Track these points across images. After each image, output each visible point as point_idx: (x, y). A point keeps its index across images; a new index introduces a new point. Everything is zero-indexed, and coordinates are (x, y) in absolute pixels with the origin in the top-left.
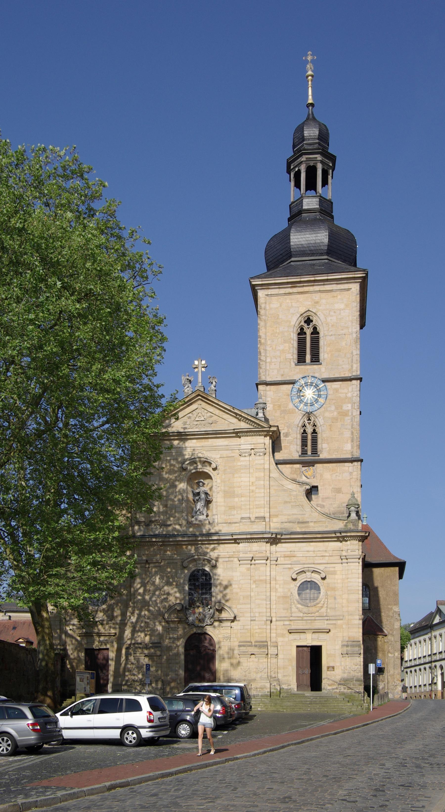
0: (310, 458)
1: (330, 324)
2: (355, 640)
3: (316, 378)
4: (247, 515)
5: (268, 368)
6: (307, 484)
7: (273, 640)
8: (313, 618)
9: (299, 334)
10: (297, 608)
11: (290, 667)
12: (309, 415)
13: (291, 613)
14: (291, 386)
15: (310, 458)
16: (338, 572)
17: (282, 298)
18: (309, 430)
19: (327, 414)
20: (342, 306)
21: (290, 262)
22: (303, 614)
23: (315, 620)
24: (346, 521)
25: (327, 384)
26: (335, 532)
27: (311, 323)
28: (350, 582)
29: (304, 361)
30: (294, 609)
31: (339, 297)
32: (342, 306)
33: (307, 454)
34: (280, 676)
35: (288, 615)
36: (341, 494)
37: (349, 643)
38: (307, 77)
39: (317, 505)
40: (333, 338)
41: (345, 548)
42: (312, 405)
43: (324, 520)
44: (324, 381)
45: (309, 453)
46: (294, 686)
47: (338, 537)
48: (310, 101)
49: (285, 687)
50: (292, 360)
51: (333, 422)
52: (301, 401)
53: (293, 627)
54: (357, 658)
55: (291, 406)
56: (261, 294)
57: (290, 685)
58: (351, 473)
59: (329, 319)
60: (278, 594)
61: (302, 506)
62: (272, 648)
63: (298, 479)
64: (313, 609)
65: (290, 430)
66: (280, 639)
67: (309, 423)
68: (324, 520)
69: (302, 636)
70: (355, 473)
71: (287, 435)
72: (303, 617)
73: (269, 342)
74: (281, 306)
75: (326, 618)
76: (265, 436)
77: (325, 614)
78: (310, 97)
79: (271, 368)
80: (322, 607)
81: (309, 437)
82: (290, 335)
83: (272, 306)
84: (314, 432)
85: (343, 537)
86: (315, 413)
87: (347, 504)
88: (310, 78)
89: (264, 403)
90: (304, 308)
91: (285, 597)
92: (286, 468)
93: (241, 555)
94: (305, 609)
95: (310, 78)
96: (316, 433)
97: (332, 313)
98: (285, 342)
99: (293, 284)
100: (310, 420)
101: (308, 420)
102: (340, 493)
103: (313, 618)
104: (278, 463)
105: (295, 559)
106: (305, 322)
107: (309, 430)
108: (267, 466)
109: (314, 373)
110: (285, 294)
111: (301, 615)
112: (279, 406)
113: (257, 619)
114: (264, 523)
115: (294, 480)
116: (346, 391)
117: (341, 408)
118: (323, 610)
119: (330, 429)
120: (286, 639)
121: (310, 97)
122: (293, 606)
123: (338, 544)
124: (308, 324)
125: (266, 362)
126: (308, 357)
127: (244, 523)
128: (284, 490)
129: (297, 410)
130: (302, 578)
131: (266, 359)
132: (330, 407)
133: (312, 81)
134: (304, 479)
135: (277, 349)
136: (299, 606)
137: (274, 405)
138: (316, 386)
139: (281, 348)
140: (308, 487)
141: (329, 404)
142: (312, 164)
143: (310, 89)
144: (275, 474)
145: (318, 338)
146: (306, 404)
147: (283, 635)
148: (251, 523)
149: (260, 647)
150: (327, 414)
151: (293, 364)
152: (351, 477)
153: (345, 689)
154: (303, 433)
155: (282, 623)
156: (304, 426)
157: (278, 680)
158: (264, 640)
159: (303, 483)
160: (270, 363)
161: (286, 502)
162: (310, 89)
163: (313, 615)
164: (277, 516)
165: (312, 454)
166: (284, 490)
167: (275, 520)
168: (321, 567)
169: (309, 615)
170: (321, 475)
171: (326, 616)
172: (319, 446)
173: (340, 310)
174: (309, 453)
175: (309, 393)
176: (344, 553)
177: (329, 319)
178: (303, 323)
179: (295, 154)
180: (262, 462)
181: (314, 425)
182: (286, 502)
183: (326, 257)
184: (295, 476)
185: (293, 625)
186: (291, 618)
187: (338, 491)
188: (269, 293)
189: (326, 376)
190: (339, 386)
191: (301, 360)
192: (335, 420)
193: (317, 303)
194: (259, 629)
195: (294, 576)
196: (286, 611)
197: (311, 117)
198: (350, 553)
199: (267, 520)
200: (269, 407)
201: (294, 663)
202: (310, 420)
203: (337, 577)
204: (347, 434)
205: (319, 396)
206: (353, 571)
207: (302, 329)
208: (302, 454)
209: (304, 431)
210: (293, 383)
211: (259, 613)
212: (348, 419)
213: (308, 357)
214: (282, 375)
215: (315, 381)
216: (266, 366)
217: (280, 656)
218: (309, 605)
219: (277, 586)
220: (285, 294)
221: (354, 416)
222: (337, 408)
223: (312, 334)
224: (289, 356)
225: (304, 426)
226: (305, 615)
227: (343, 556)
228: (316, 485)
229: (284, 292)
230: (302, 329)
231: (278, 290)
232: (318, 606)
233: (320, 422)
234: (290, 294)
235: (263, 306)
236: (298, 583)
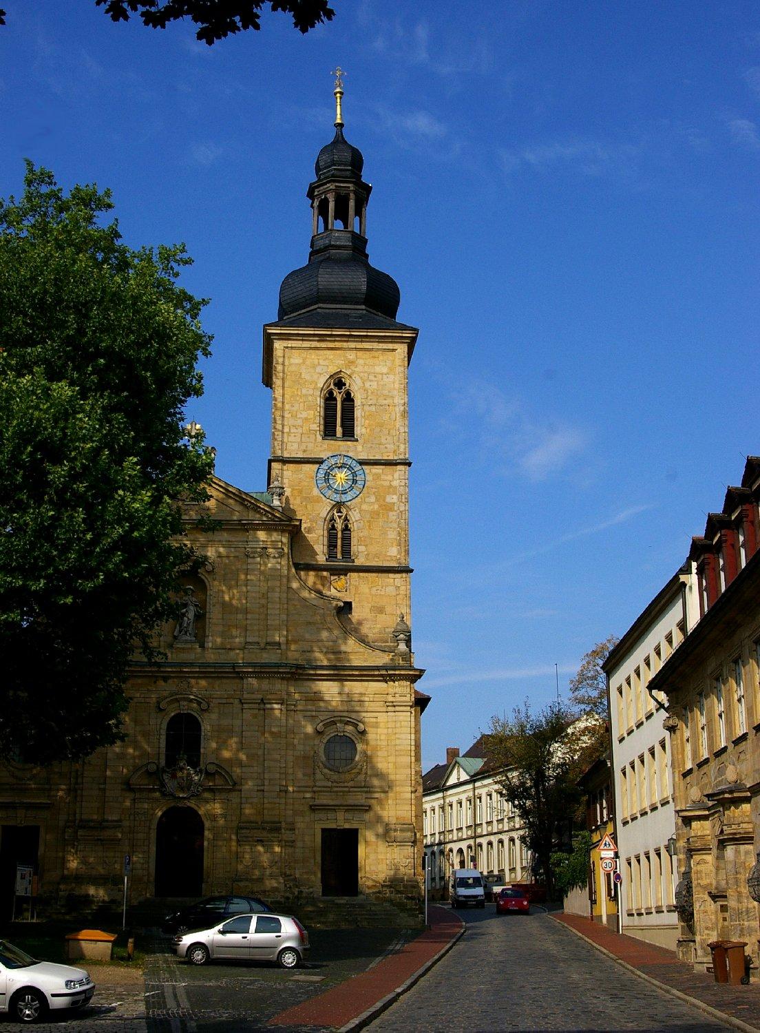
0: (341, 563)
1: (370, 391)
2: (406, 822)
3: (351, 458)
4: (256, 639)
5: (285, 440)
6: (339, 600)
7: (290, 820)
8: (347, 789)
10: (324, 775)
11: (312, 861)
12: (339, 506)
13: (314, 781)
14: (317, 466)
15: (341, 563)
16: (382, 725)
17: (304, 354)
19: (364, 507)
21: (316, 309)
22: (332, 782)
23: (349, 792)
24: (393, 654)
25: (364, 467)
26: (378, 668)
27: (344, 387)
28: (399, 739)
30: (319, 776)
33: (336, 557)
35: (311, 784)
36: (383, 615)
37: (397, 826)
38: (336, 94)
41: (391, 691)
42: (344, 492)
43: (362, 650)
44: (362, 463)
45: (339, 556)
46: (318, 889)
47: (382, 675)
48: (339, 121)
50: (318, 432)
51: (372, 518)
53: (317, 802)
54: (409, 848)
55: (316, 492)
56: (278, 345)
57: (312, 888)
58: (398, 588)
60: (298, 754)
62: (288, 832)
63: (324, 592)
64: (348, 776)
65: (314, 525)
66: (298, 819)
67: (340, 517)
68: (362, 650)
69: (331, 815)
70: (403, 588)
71: (309, 530)
72: (331, 787)
73: (287, 407)
74: (304, 363)
75: (366, 789)
77: (363, 784)
78: (339, 116)
79: (290, 440)
80: (359, 773)
81: (339, 535)
82: (316, 400)
83: (292, 361)
84: (346, 529)
85: (390, 675)
86: (349, 503)
87: (393, 630)
88: (338, 95)
89: (280, 488)
90: (336, 368)
91: (305, 758)
93: (245, 696)
94: (335, 777)
95: (338, 95)
96: (350, 530)
97: (371, 377)
98: (309, 408)
99: (322, 338)
100: (342, 512)
101: (337, 512)
102: (382, 613)
103: (347, 789)
106: (335, 385)
107: (339, 525)
109: (348, 451)
110: (311, 348)
111: (330, 784)
112: (300, 492)
113: (266, 788)
114: (279, 651)
116: (390, 477)
117: (384, 501)
118: (362, 777)
119: (369, 526)
121: (339, 116)
122: (318, 771)
123: (383, 685)
124: (340, 388)
125: (283, 433)
126: (339, 430)
127: (251, 650)
129: (324, 498)
130: (331, 732)
131: (283, 428)
132: (368, 497)
133: (341, 98)
135: (298, 417)
136: (326, 771)
137: (293, 489)
138: (350, 468)
139: (304, 415)
141: (368, 493)
142: (343, 192)
143: (338, 107)
145: (353, 407)
146: (336, 491)
148: (260, 651)
149: (272, 830)
150: (364, 507)
151: (319, 438)
152: (398, 593)
153: (391, 892)
154: (331, 530)
158: (277, 820)
160: (289, 433)
162: (338, 107)
163: (346, 784)
165: (343, 558)
167: (293, 647)
169: (341, 784)
170: (357, 588)
171: (364, 787)
172: (354, 549)
174: (339, 556)
175: (341, 477)
176: (390, 698)
177: (367, 384)
178: (332, 386)
179: (319, 180)
181: (346, 519)
183: (363, 307)
185: (318, 799)
186: (315, 789)
187: (381, 610)
188: (289, 346)
189: (363, 456)
190: (381, 471)
191: (329, 432)
192: (375, 515)
193: (352, 362)
194: (269, 803)
196: (306, 778)
197: (340, 138)
198: (398, 699)
199: (283, 647)
200: (288, 492)
202: (342, 512)
203: (379, 730)
204: (392, 535)
205: (354, 481)
206: (403, 723)
207: (331, 393)
208: (329, 557)
209: (333, 526)
210: (320, 462)
211: (270, 780)
212: (393, 516)
213: (339, 430)
214: (304, 451)
215: (349, 462)
216: (283, 437)
217: (299, 844)
218: (341, 771)
220: (311, 348)
221: (401, 512)
222: (377, 500)
223: (343, 401)
224: (315, 427)
225: (332, 519)
226: (335, 784)
227: (389, 702)
228: (349, 600)
229: (309, 346)
230: (331, 393)
231: (301, 342)
232: (353, 771)
235: (280, 360)
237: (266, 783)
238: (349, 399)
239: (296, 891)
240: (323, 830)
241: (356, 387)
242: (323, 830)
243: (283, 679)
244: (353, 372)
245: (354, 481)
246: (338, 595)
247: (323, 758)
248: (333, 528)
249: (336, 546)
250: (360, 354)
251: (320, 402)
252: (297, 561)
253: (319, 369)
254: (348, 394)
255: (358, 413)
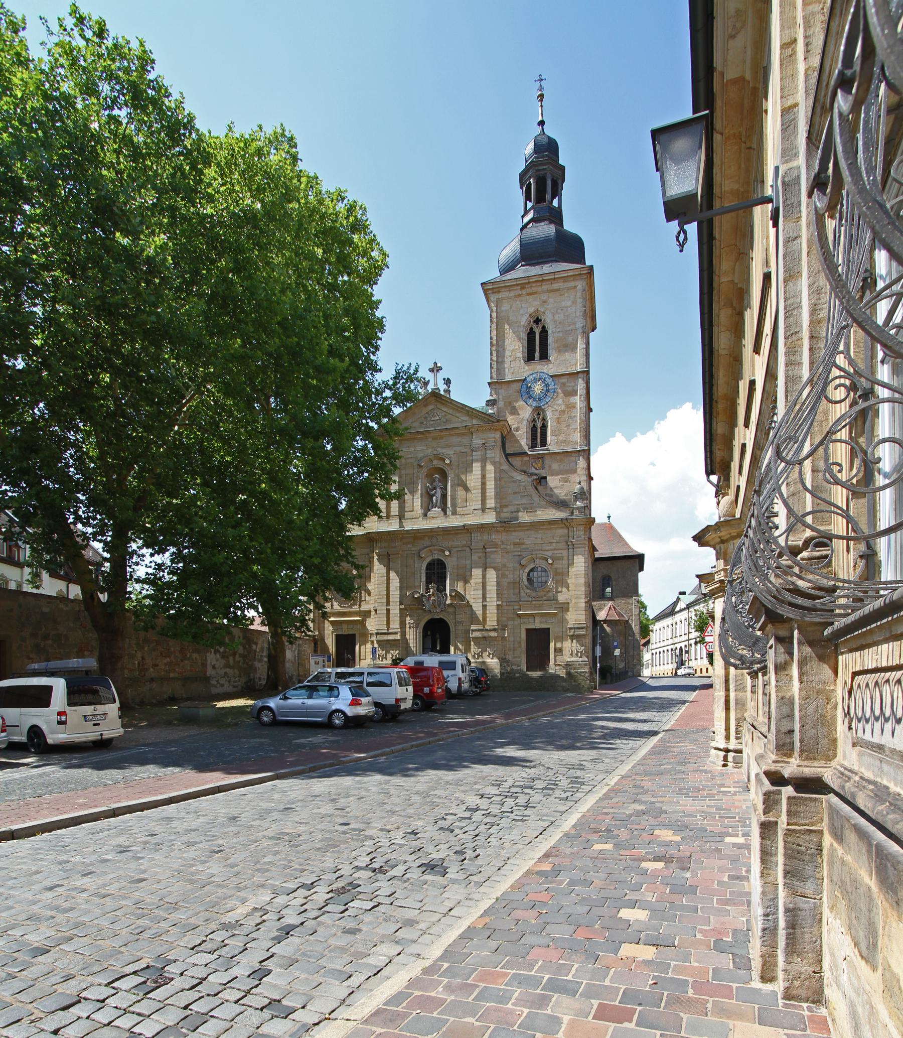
6: (536, 474)
9: (529, 334)
18: (539, 424)
20: (569, 303)
29: (534, 360)
30: (523, 594)
31: (566, 295)
32: (569, 303)
34: (509, 657)
35: (517, 599)
39: (546, 495)
40: (561, 334)
42: (540, 399)
44: (552, 376)
49: (515, 668)
52: (530, 397)
59: (556, 317)
61: (531, 496)
64: (542, 594)
69: (531, 620)
71: (517, 429)
76: (496, 430)
81: (539, 431)
83: (503, 308)
91: (514, 583)
92: (517, 461)
94: (534, 594)
97: (559, 311)
104: (507, 456)
105: (524, 546)
106: (534, 322)
107: (539, 424)
108: (497, 459)
110: (515, 296)
115: (525, 472)
120: (516, 623)
124: (537, 324)
126: (537, 355)
128: (514, 482)
134: (534, 471)
136: (528, 591)
140: (535, 477)
144: (505, 467)
145: (547, 336)
147: (513, 619)
151: (523, 362)
155: (511, 608)
156: (534, 420)
157: (508, 662)
159: (532, 474)
161: (515, 493)
164: (507, 506)
166: (514, 482)
167: (505, 510)
168: (549, 553)
170: (550, 466)
173: (567, 307)
177: (556, 317)
180: (493, 455)
182: (515, 493)
184: (525, 468)
191: (530, 357)
193: (545, 302)
195: (523, 562)
201: (524, 645)
207: (531, 329)
213: (537, 355)
215: (544, 376)
219: (507, 573)
223: (541, 333)
224: (520, 355)
225: (534, 420)
230: (531, 329)
233: (549, 415)
234: (520, 295)
236: (527, 570)
237: (488, 600)
238: (544, 332)
239: (509, 669)
240: (528, 630)
241: (548, 320)
242: (528, 630)
243: (498, 531)
244: (547, 309)
245: (548, 391)
246: (537, 472)
247: (526, 582)
248: (534, 427)
249: (536, 439)
250: (551, 295)
251: (524, 336)
252: (508, 451)
253: (521, 312)
254: (544, 327)
255: (550, 340)
